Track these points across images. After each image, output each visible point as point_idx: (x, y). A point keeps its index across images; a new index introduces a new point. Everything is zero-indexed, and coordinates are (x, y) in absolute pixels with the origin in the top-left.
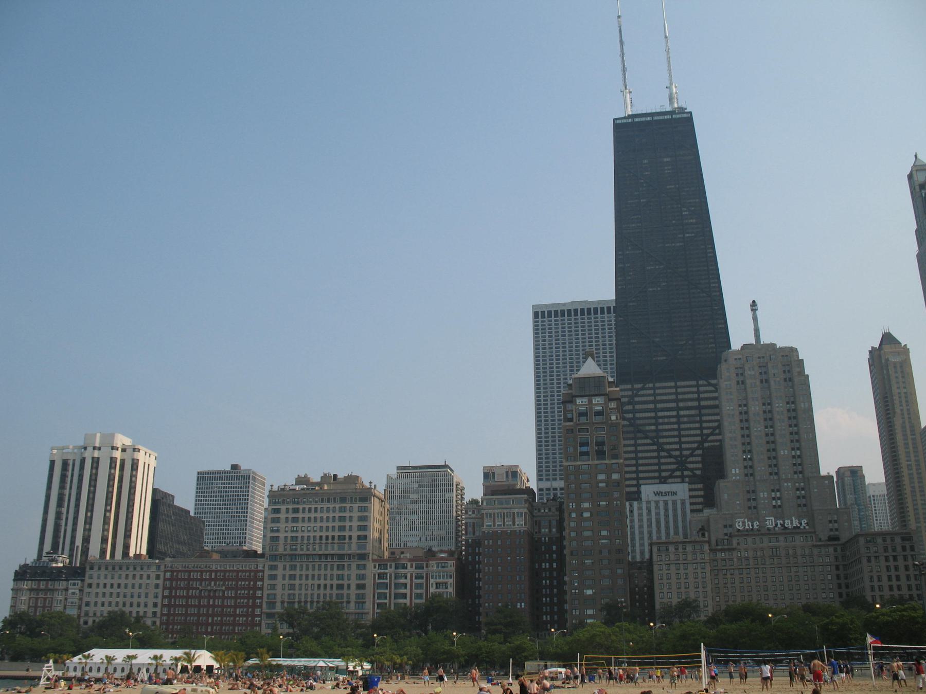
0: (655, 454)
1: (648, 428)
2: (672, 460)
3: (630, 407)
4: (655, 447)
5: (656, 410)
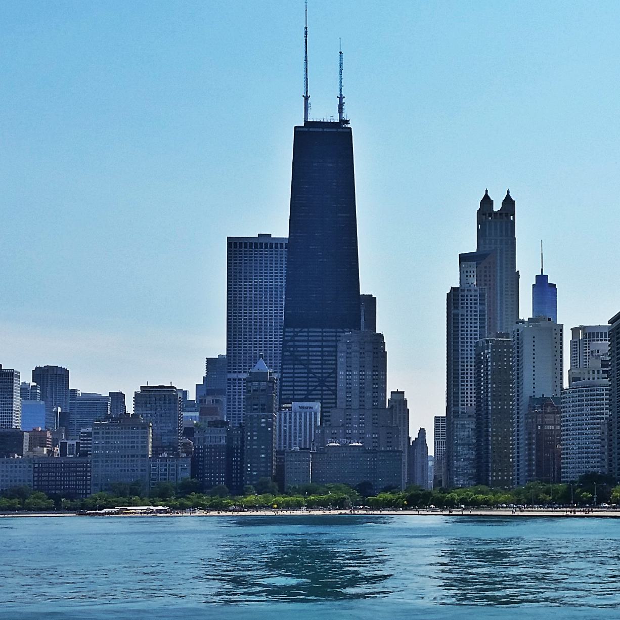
0: (306, 375)
1: (302, 358)
2: (316, 380)
3: (291, 344)
4: (306, 371)
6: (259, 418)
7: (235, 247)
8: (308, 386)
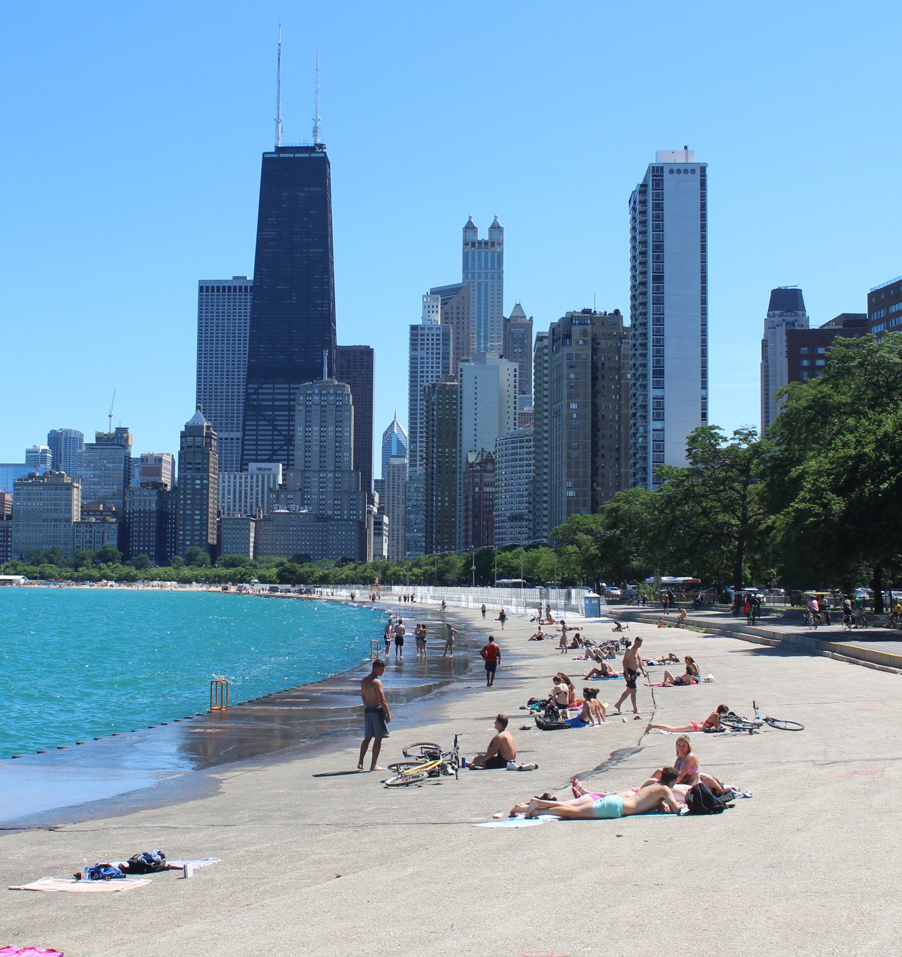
0: (270, 433)
1: (266, 413)
2: (282, 438)
3: (255, 397)
4: (271, 428)
5: (274, 400)
6: (194, 479)
7: (207, 291)
8: (273, 445)
